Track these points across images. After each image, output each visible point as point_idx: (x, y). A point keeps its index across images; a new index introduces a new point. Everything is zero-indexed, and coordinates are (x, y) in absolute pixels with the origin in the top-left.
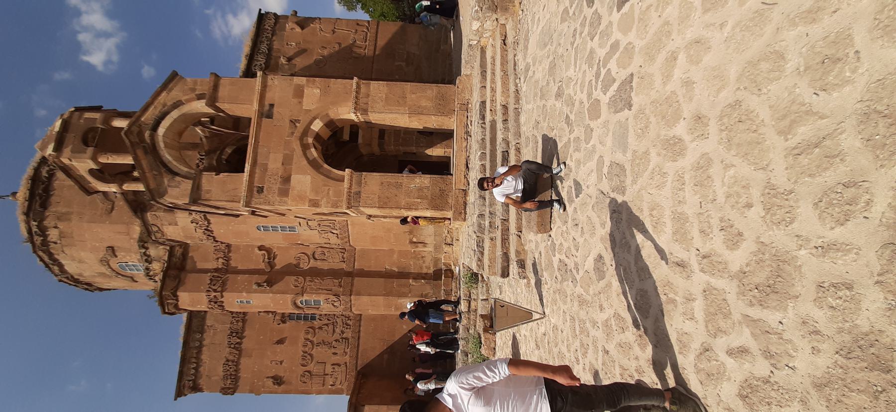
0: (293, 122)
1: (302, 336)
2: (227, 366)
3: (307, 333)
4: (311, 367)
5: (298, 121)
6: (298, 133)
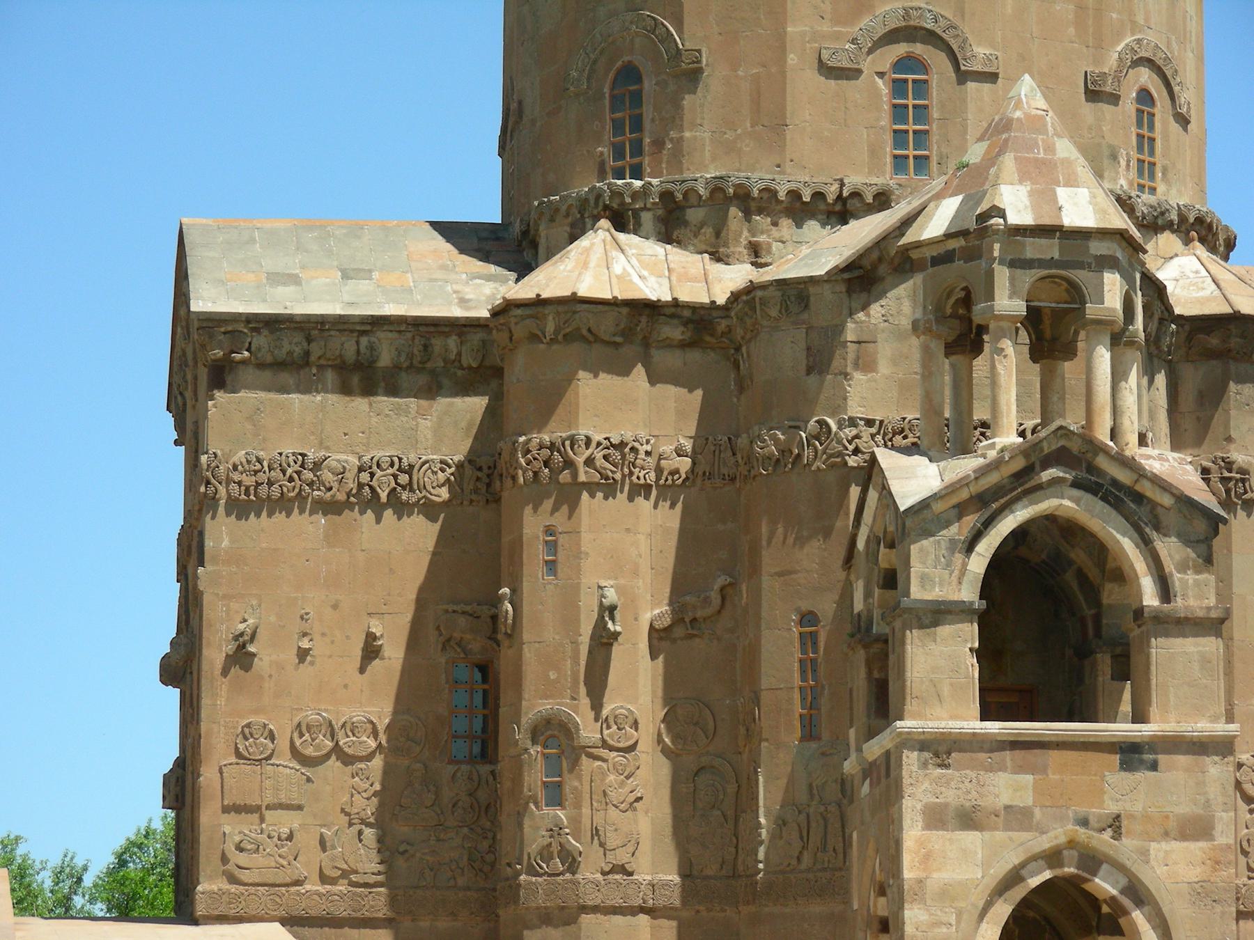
0: (1115, 825)
2: (297, 467)
5: (1117, 835)
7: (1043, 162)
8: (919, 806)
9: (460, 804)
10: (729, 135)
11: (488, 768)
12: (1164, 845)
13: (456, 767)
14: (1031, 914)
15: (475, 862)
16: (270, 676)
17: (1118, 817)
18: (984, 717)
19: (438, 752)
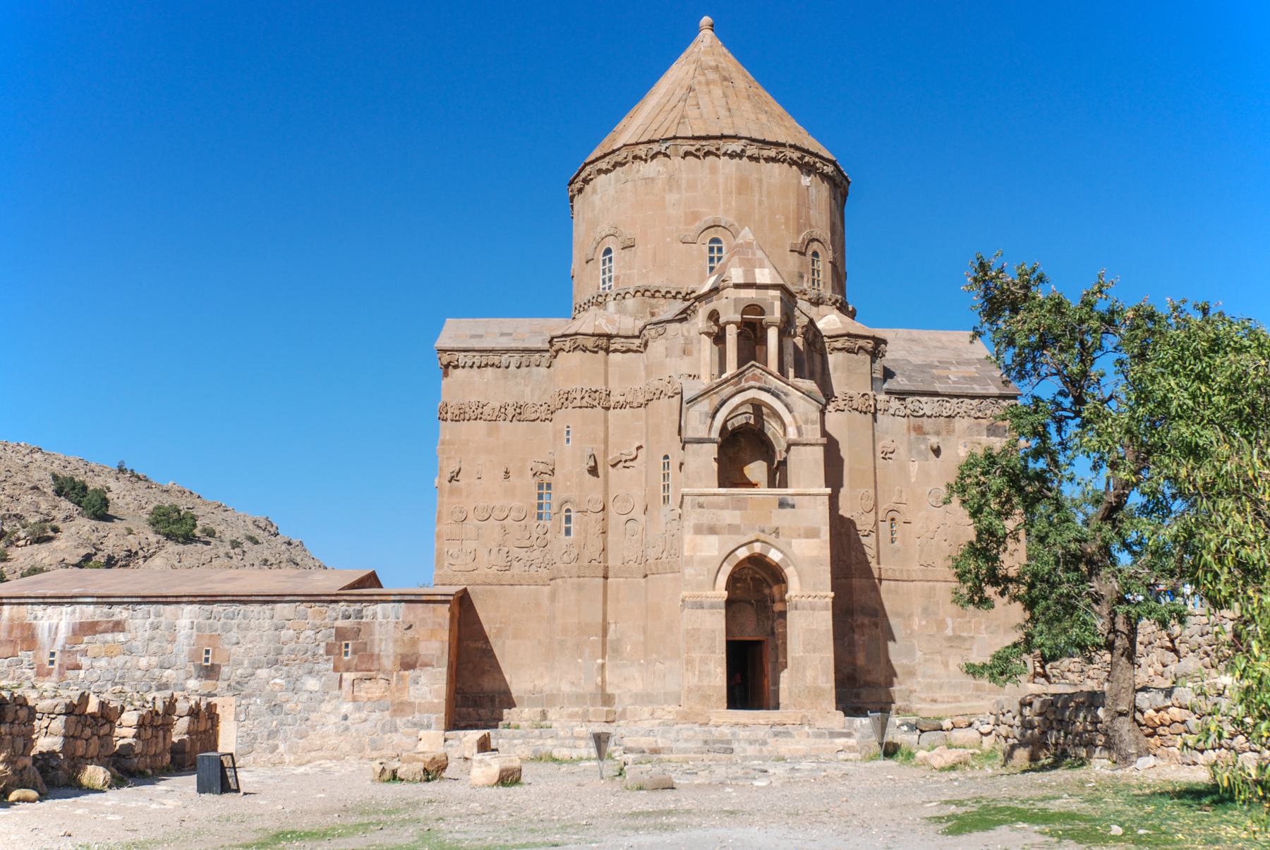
0: (776, 532)
1: (516, 504)
3: (519, 510)
4: (473, 521)
5: (777, 536)
6: (762, 537)
7: (751, 259)
8: (692, 524)
10: (644, 271)
12: (798, 540)
14: (758, 576)
17: (777, 529)
18: (720, 486)
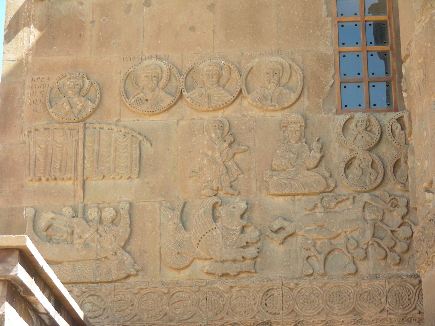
9: (356, 162)
11: (393, 115)
13: (348, 117)
15: (382, 239)
16: (93, 22)
19: (321, 100)
